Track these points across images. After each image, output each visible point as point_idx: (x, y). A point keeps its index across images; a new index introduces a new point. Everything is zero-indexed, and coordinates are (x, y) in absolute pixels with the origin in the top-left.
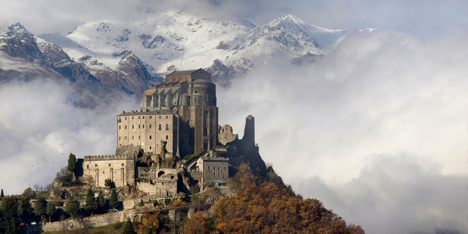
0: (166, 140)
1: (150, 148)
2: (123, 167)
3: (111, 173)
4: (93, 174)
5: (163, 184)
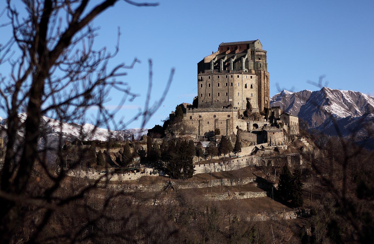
0: (250, 97)
2: (229, 118)
5: (274, 133)
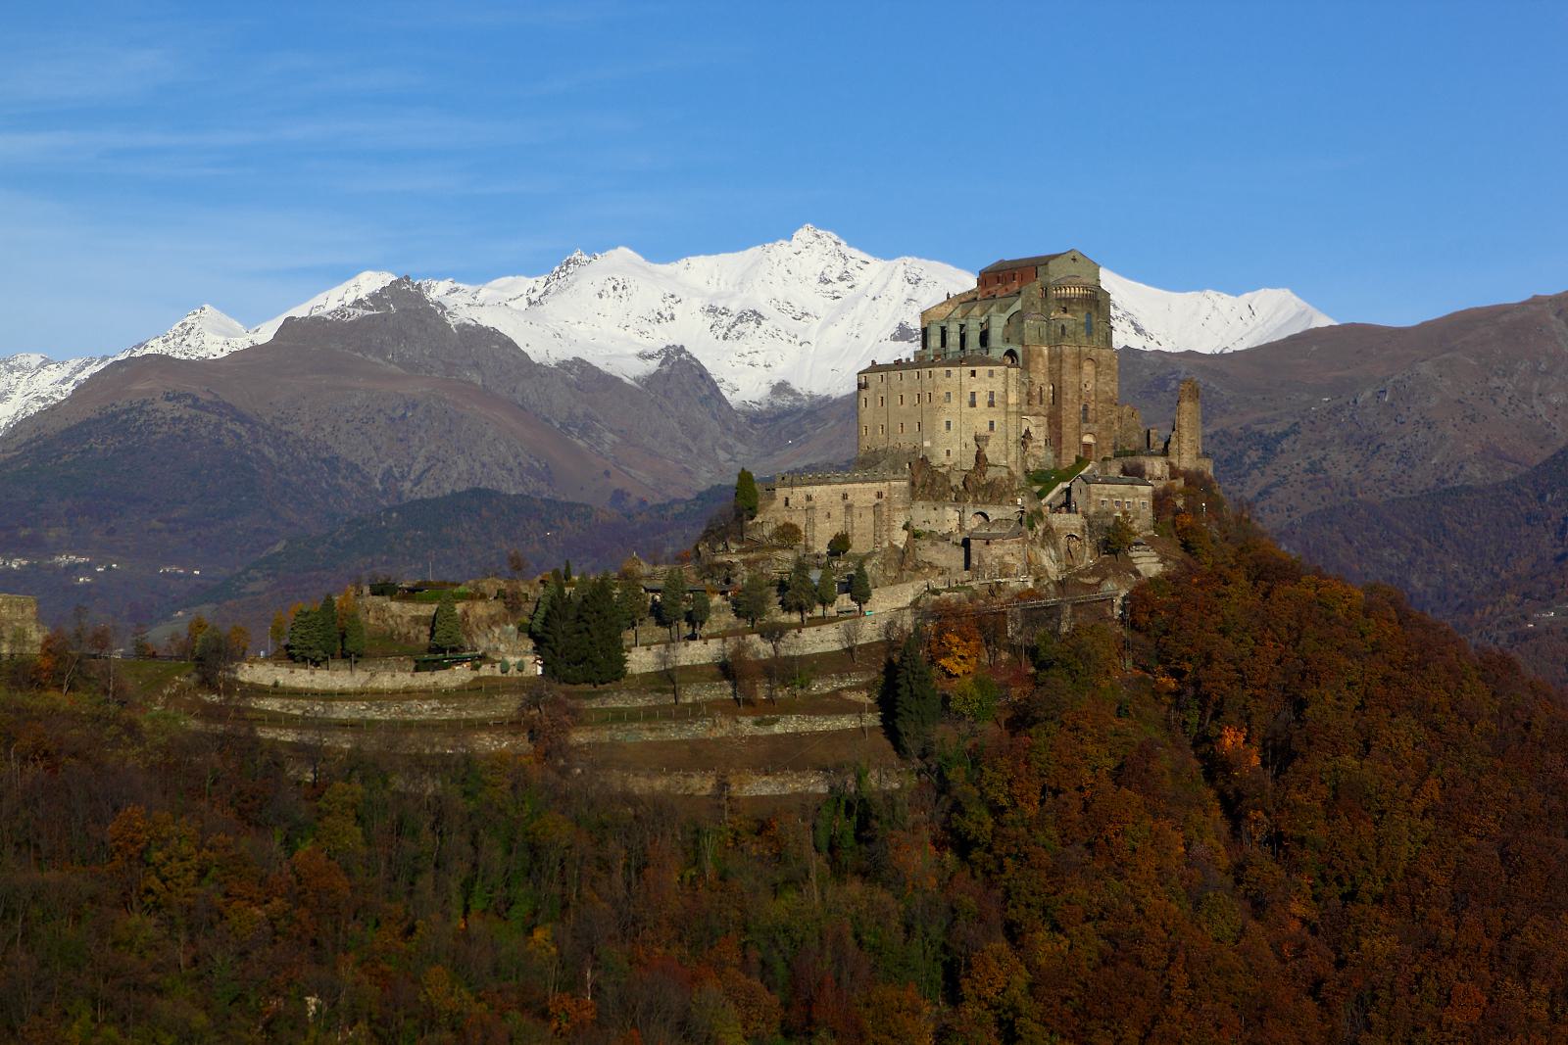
1: (948, 452)
3: (849, 520)
4: (798, 520)
5: (988, 543)
